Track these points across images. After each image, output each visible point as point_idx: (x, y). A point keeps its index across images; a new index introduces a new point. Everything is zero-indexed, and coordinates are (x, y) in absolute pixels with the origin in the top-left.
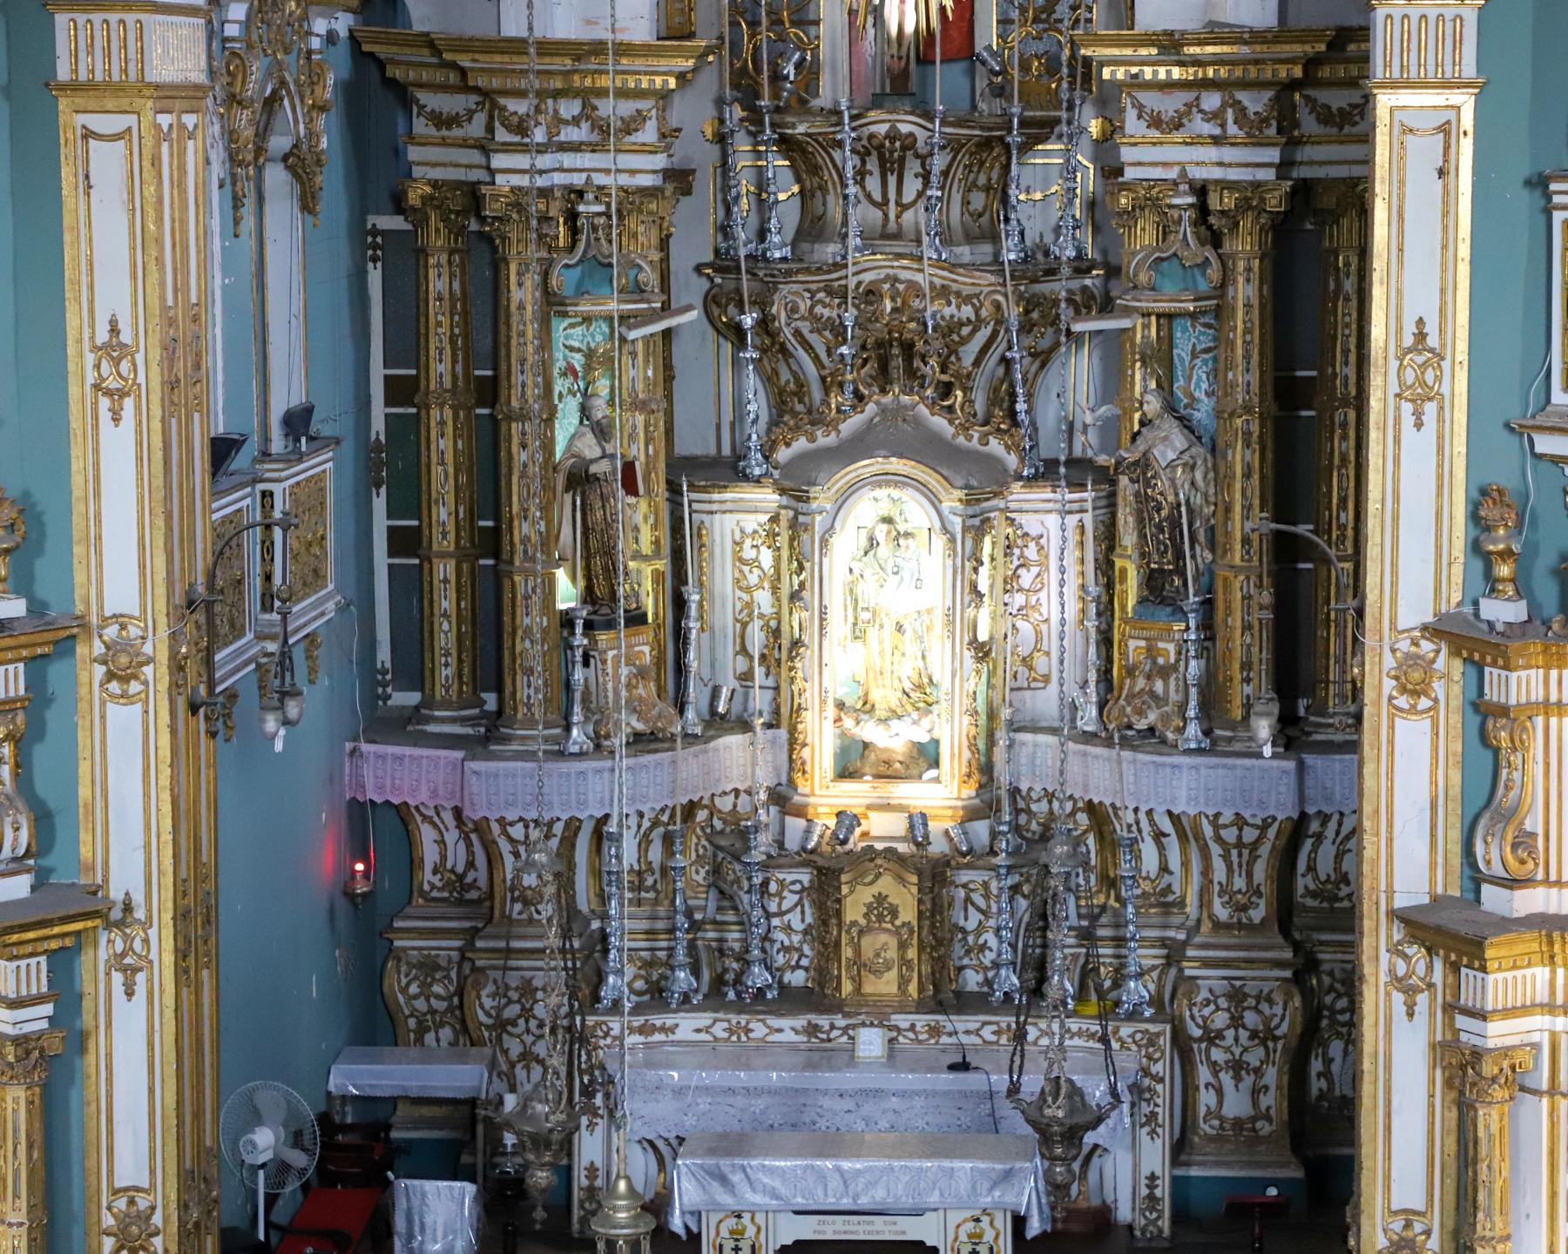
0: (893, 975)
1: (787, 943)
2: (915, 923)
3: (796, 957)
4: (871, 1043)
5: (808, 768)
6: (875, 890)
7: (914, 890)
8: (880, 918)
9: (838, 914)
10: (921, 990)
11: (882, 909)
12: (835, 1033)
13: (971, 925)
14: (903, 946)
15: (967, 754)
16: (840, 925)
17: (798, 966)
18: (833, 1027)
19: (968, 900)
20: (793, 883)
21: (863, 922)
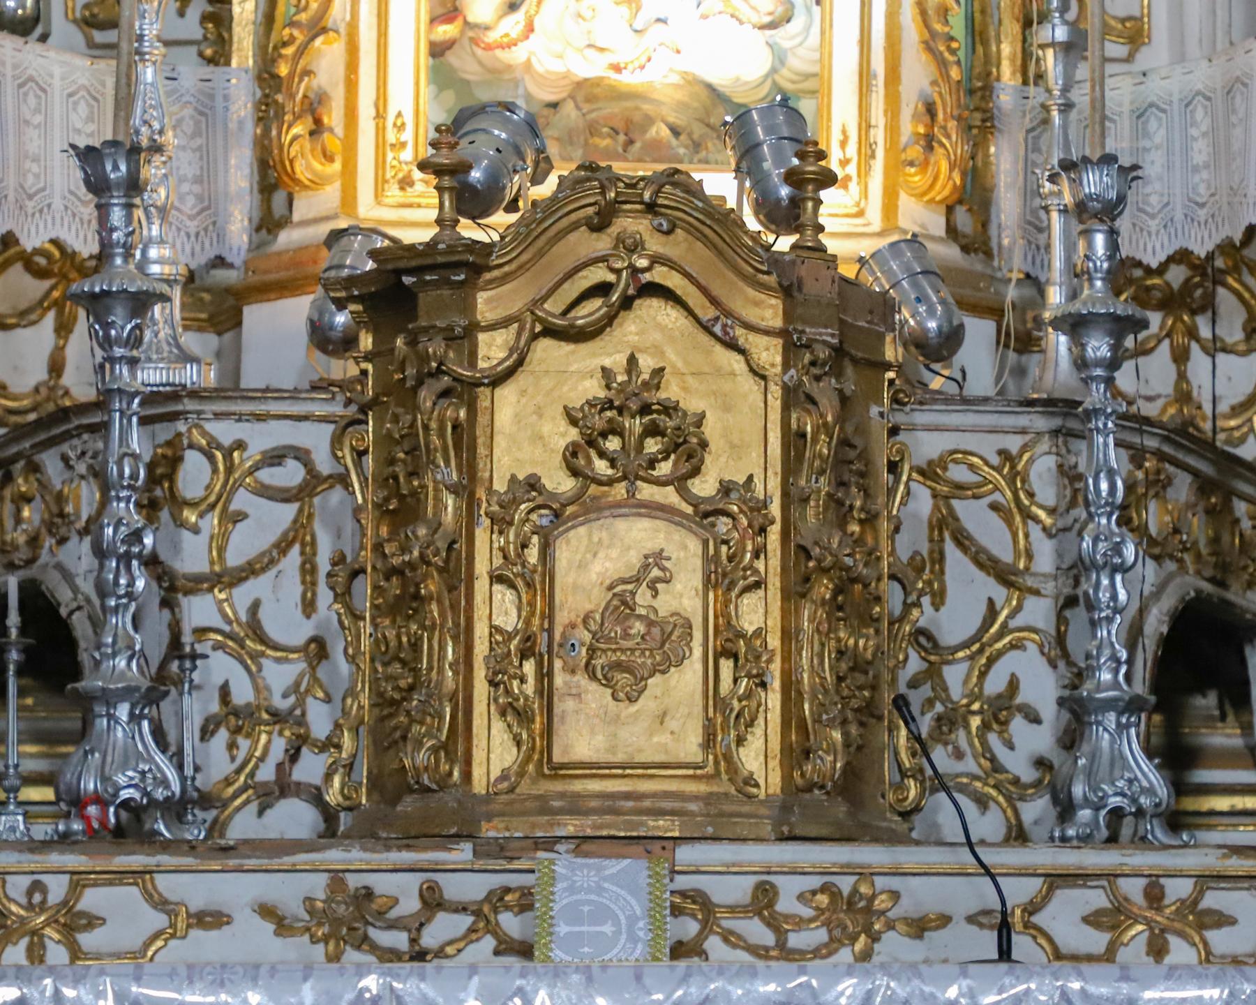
0: (686, 680)
1: (243, 694)
2: (770, 487)
3: (279, 747)
4: (602, 914)
5: (334, 117)
6: (608, 353)
7: (769, 353)
8: (633, 470)
9: (465, 441)
10: (797, 752)
11: (637, 433)
12: (442, 928)
13: (955, 619)
14: (723, 578)
15: (918, 75)
16: (466, 490)
17: (283, 787)
18: (433, 902)
19: (945, 525)
20: (275, 458)
21: (561, 483)
